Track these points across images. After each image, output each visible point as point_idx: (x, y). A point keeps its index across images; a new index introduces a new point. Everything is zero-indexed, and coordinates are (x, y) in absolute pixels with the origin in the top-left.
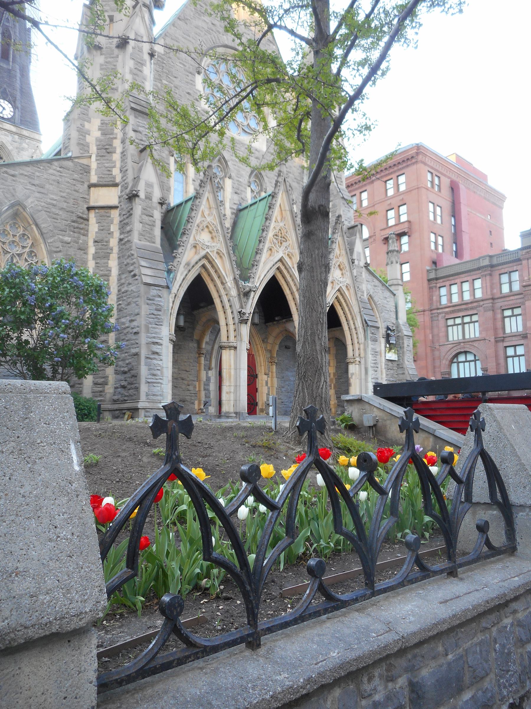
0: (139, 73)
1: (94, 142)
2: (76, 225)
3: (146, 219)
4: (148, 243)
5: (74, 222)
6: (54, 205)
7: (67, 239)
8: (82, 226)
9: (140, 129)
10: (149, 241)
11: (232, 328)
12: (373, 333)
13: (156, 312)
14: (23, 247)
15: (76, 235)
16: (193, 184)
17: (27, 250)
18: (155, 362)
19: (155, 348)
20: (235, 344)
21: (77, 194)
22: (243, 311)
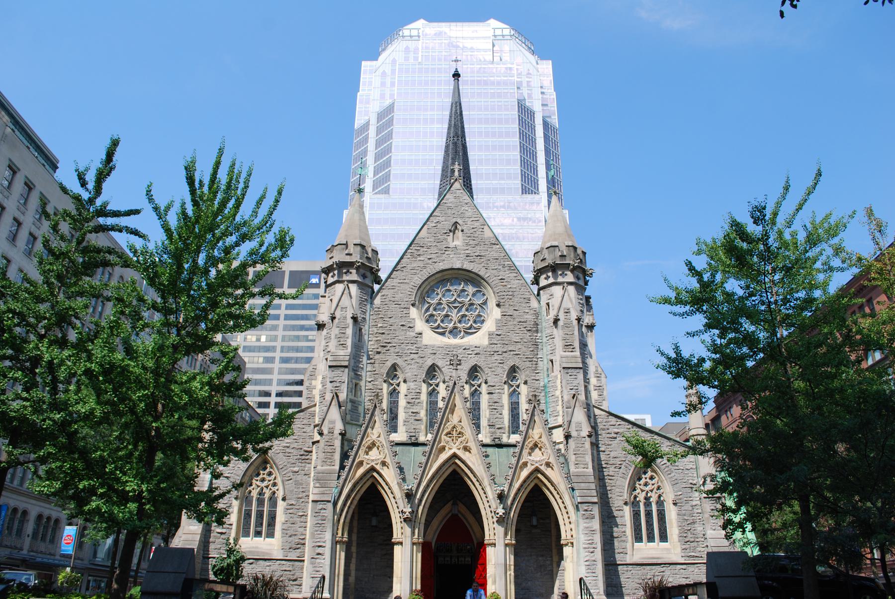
0: (342, 335)
1: (318, 393)
2: (303, 457)
3: (329, 449)
4: (328, 467)
5: (302, 455)
6: (288, 447)
7: (296, 469)
8: (307, 457)
9: (335, 379)
10: (330, 465)
11: (399, 524)
12: (586, 510)
13: (320, 522)
14: (269, 481)
15: (303, 465)
16: (406, 399)
17: (272, 482)
18: (318, 561)
19: (320, 550)
20: (401, 540)
21: (305, 434)
22: (404, 510)
